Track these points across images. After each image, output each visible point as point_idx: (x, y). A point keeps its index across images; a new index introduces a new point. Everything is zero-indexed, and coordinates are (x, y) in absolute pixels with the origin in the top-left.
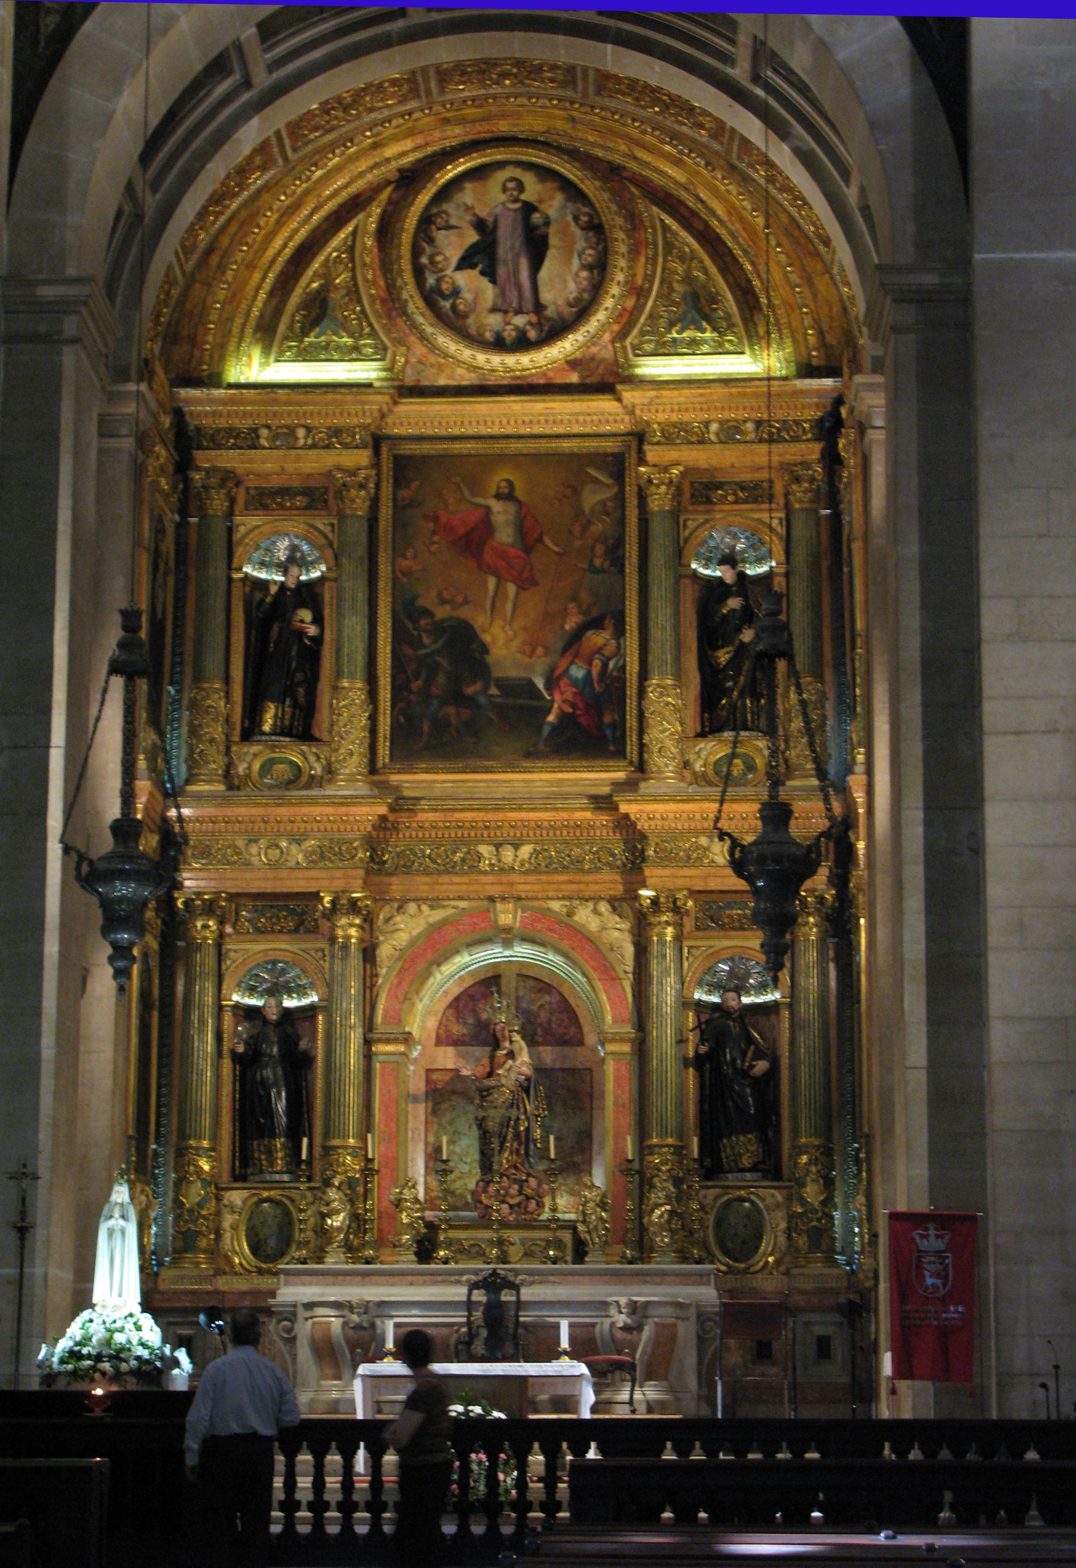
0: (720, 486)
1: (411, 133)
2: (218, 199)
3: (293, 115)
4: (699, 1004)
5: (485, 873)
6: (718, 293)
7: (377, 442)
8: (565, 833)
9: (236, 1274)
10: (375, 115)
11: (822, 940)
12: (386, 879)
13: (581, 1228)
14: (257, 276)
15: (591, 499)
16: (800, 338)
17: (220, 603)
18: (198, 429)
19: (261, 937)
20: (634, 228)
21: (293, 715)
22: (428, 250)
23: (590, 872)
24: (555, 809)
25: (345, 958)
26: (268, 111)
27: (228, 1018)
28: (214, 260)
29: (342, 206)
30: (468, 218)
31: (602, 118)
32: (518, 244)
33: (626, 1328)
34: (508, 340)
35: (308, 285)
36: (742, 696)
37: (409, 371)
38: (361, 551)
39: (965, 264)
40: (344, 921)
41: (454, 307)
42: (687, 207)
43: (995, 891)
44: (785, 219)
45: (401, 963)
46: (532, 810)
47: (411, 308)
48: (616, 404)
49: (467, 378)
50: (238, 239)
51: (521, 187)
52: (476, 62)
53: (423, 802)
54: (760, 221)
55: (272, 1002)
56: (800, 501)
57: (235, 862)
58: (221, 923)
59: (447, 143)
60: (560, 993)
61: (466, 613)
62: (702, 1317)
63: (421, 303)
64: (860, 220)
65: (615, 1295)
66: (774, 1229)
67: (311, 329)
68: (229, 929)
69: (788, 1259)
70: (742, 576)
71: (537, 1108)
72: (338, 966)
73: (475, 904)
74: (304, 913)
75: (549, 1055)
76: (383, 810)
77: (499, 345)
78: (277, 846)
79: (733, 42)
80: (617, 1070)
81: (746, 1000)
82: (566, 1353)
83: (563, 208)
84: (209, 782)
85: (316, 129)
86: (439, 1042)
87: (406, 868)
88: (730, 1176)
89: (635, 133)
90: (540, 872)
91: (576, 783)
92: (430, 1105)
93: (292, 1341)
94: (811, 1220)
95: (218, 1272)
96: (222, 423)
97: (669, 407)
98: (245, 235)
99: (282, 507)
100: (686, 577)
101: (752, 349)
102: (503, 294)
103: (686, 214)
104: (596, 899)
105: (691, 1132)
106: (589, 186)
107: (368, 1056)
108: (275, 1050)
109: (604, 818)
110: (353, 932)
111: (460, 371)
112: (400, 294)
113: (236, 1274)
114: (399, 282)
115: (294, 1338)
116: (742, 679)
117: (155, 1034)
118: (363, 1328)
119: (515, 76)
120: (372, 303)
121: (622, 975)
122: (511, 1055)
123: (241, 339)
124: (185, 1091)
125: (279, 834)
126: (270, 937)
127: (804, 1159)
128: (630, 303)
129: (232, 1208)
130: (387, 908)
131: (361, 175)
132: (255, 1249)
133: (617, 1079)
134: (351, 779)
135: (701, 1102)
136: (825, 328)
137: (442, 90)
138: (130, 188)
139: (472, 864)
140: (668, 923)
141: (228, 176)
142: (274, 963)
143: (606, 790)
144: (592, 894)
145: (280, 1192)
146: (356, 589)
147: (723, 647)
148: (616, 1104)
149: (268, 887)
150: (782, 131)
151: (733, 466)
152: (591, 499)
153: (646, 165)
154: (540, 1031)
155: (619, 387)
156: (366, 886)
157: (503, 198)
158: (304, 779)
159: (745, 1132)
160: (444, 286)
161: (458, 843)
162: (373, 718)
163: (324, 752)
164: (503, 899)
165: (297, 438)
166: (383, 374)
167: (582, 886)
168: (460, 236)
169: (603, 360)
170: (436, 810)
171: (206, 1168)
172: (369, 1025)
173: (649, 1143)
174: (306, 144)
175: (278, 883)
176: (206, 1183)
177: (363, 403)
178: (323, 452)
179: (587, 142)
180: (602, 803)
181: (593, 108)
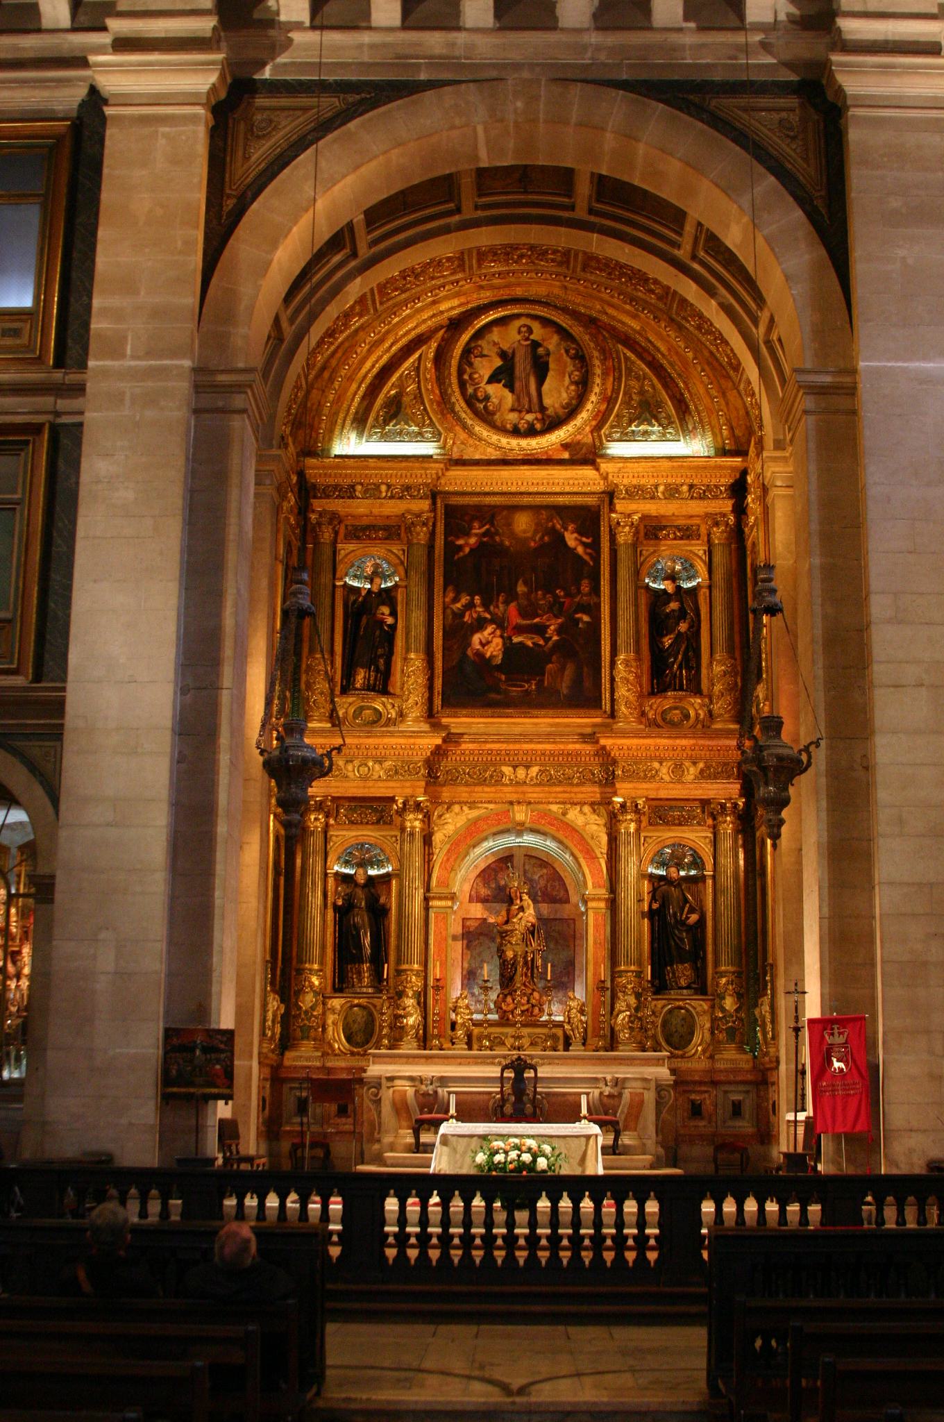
0: (665, 528)
1: (457, 295)
2: (331, 333)
3: (382, 279)
4: (651, 877)
5: (506, 785)
6: (661, 402)
7: (434, 495)
8: (561, 759)
9: (336, 1055)
10: (433, 282)
11: (737, 831)
12: (439, 789)
13: (567, 1027)
14: (354, 386)
16: (717, 432)
17: (328, 601)
18: (314, 486)
19: (354, 827)
20: (605, 359)
21: (376, 677)
22: (468, 370)
23: (577, 785)
24: (554, 743)
25: (411, 842)
26: (368, 273)
27: (331, 881)
28: (326, 375)
29: (411, 341)
30: (496, 350)
31: (585, 287)
32: (528, 367)
33: (610, 1096)
34: (522, 430)
35: (389, 392)
36: (680, 668)
37: (455, 449)
38: (423, 568)
39: (853, 372)
40: (411, 816)
41: (486, 407)
42: (640, 345)
43: (883, 795)
44: (706, 354)
45: (448, 846)
46: (539, 742)
47: (457, 408)
48: (594, 472)
49: (494, 454)
51: (530, 331)
52: (504, 246)
53: (465, 736)
54: (690, 355)
55: (361, 871)
56: (719, 539)
57: (337, 776)
58: (327, 816)
59: (481, 302)
60: (554, 868)
62: (660, 1088)
63: (463, 404)
65: (603, 1073)
66: (702, 1027)
67: (390, 420)
68: (332, 821)
69: (711, 1048)
70: (679, 588)
71: (539, 945)
72: (407, 847)
73: (499, 806)
74: (383, 811)
75: (545, 909)
76: (439, 741)
77: (516, 432)
78: (366, 765)
79: (680, 235)
80: (596, 920)
81: (682, 873)
82: (585, 1118)
83: (558, 345)
84: (320, 721)
85: (396, 290)
86: (471, 901)
87: (453, 781)
88: (672, 992)
89: (605, 296)
90: (544, 785)
91: (568, 725)
92: (465, 942)
93: (378, 1102)
94: (728, 1022)
95: (325, 1054)
96: (330, 481)
97: (631, 475)
98: (347, 358)
99: (370, 538)
100: (642, 588)
101: (684, 437)
102: (518, 399)
103: (640, 350)
104: (582, 804)
105: (646, 963)
106: (577, 330)
107: (427, 909)
108: (363, 904)
109: (588, 748)
110: (417, 824)
111: (489, 450)
112: (450, 399)
113: (336, 1055)
114: (449, 391)
115: (380, 1099)
116: (680, 657)
117: (282, 892)
118: (429, 1095)
119: (530, 257)
120: (431, 405)
121: (599, 855)
122: (522, 909)
123: (343, 427)
125: (367, 757)
126: (360, 827)
127: (724, 980)
128: (603, 407)
129: (333, 1010)
130: (440, 808)
131: (424, 321)
132: (349, 1039)
133: (596, 926)
134: (416, 720)
135: (652, 942)
136: (734, 424)
137: (479, 266)
138: (277, 321)
139: (497, 780)
140: (632, 820)
141: (338, 318)
142: (363, 845)
143: (589, 730)
144: (579, 800)
145: (366, 1000)
146: (418, 590)
147: (666, 635)
148: (595, 943)
149: (360, 793)
150: (711, 292)
151: (673, 515)
153: (613, 318)
154: (539, 894)
155: (598, 460)
156: (425, 793)
157: (519, 337)
158: (383, 720)
159: (682, 963)
160: (479, 394)
162: (431, 680)
163: (397, 702)
164: (519, 803)
165: (381, 492)
166: (438, 451)
167: (573, 795)
168: (491, 361)
169: (585, 444)
170: (474, 742)
171: (317, 983)
172: (428, 889)
173: (618, 969)
174: (388, 300)
175: (366, 790)
176: (316, 994)
177: (426, 469)
178: (398, 502)
179: (574, 303)
180: (590, 738)
181: (579, 280)
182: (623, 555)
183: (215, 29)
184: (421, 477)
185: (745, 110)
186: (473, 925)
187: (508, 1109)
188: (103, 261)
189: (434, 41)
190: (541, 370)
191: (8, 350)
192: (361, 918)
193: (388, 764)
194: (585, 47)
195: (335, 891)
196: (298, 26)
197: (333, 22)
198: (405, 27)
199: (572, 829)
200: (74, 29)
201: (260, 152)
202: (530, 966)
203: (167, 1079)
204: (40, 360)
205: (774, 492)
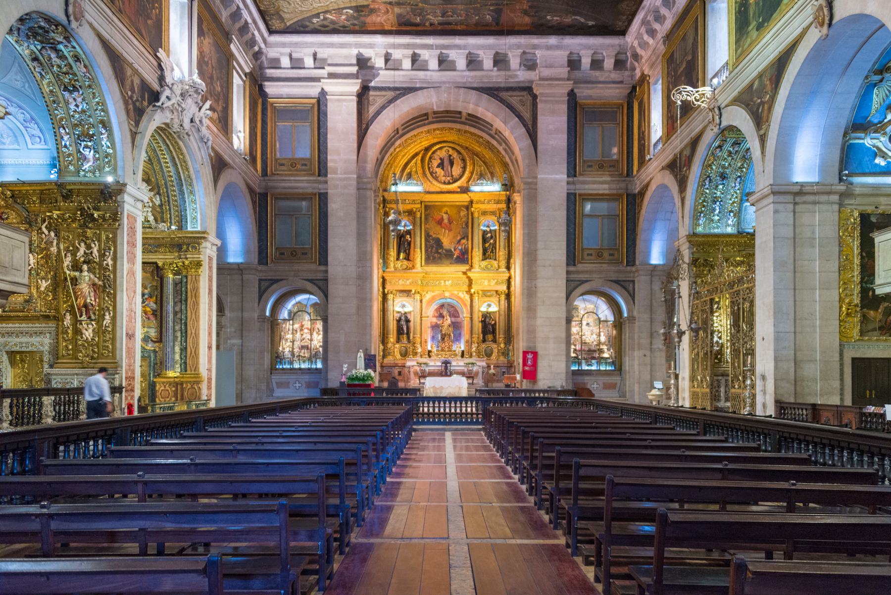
1: (427, 140)
15: (463, 213)
39: (536, 178)
43: (539, 295)
49: (438, 190)
50: (394, 161)
61: (438, 236)
64: (515, 163)
75: (453, 319)
77: (445, 183)
87: (427, 284)
106: (462, 151)
109: (465, 276)
124: (388, 327)
132: (401, 355)
150: (501, 145)
152: (463, 213)
161: (437, 280)
180: (465, 273)
182: (476, 220)
183: (357, 71)
184: (417, 198)
185: (511, 96)
186: (434, 324)
187: (444, 373)
188: (330, 145)
189: (421, 74)
190: (452, 163)
192: (403, 323)
193: (410, 281)
194: (463, 77)
195: (397, 316)
196: (381, 69)
197: (392, 67)
198: (412, 70)
199: (459, 298)
200: (315, 68)
201: (372, 110)
202: (450, 335)
204: (313, 174)
205: (517, 205)
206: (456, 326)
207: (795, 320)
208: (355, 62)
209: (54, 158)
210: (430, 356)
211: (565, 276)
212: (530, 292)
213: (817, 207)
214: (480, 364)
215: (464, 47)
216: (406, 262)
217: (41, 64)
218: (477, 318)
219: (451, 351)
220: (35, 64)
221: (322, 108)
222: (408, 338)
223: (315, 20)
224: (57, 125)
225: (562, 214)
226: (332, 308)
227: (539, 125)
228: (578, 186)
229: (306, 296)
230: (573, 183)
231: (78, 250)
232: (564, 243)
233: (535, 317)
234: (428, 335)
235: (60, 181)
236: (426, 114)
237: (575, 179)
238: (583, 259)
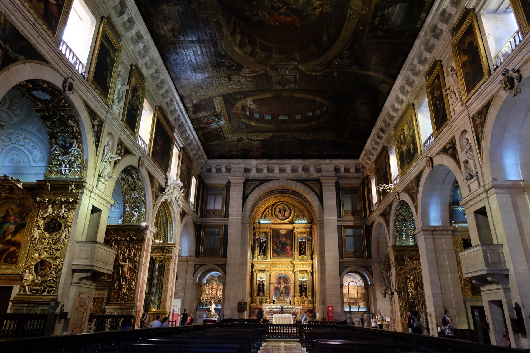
39: (323, 218)
43: (327, 273)
49: (278, 222)
62: (300, 310)
75: (286, 285)
77: (281, 220)
106: (290, 206)
150: (307, 203)
180: (291, 262)
186: (276, 287)
189: (271, 175)
190: (285, 211)
191: (219, 215)
192: (261, 286)
195: (258, 283)
200: (226, 172)
203: (239, 309)
204: (222, 217)
206: (287, 288)
207: (441, 287)
208: (243, 170)
209: (122, 215)
210: (274, 304)
211: (338, 264)
212: (322, 271)
213: (443, 236)
214: (298, 308)
215: (290, 164)
216: (263, 256)
217: (125, 181)
218: (297, 284)
219: (284, 301)
220: (123, 181)
221: (228, 188)
222: (264, 294)
223: (227, 154)
224: (125, 202)
225: (336, 235)
226: (229, 278)
227: (323, 195)
228: (342, 222)
229: (216, 272)
230: (340, 221)
231: (126, 253)
232: (338, 249)
233: (325, 284)
234: (273, 293)
235: (123, 225)
236: (274, 191)
237: (341, 219)
238: (347, 256)
